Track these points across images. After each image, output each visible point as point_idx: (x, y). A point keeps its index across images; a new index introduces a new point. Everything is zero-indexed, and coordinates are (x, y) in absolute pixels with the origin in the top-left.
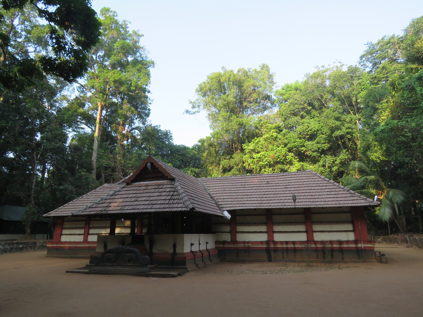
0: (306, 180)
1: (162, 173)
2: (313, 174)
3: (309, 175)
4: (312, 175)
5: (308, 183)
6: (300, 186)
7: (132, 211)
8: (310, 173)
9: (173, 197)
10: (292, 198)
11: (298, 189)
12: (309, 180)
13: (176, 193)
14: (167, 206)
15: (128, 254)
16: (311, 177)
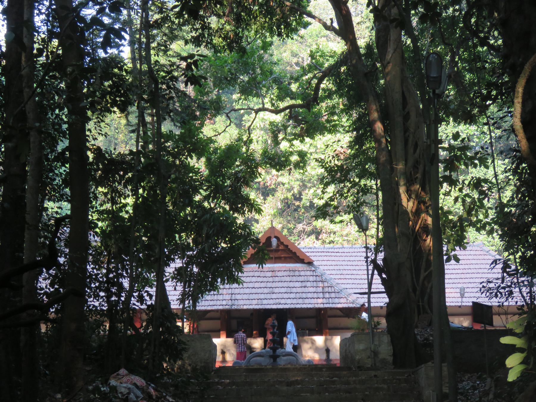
0: (473, 262)
1: (295, 253)
2: (485, 251)
3: (477, 253)
4: (482, 253)
5: (477, 266)
6: (464, 271)
7: (274, 307)
8: (479, 249)
9: (326, 290)
10: (458, 290)
11: (463, 276)
12: (478, 262)
13: (326, 284)
14: (325, 301)
15: (285, 358)
16: (481, 257)
